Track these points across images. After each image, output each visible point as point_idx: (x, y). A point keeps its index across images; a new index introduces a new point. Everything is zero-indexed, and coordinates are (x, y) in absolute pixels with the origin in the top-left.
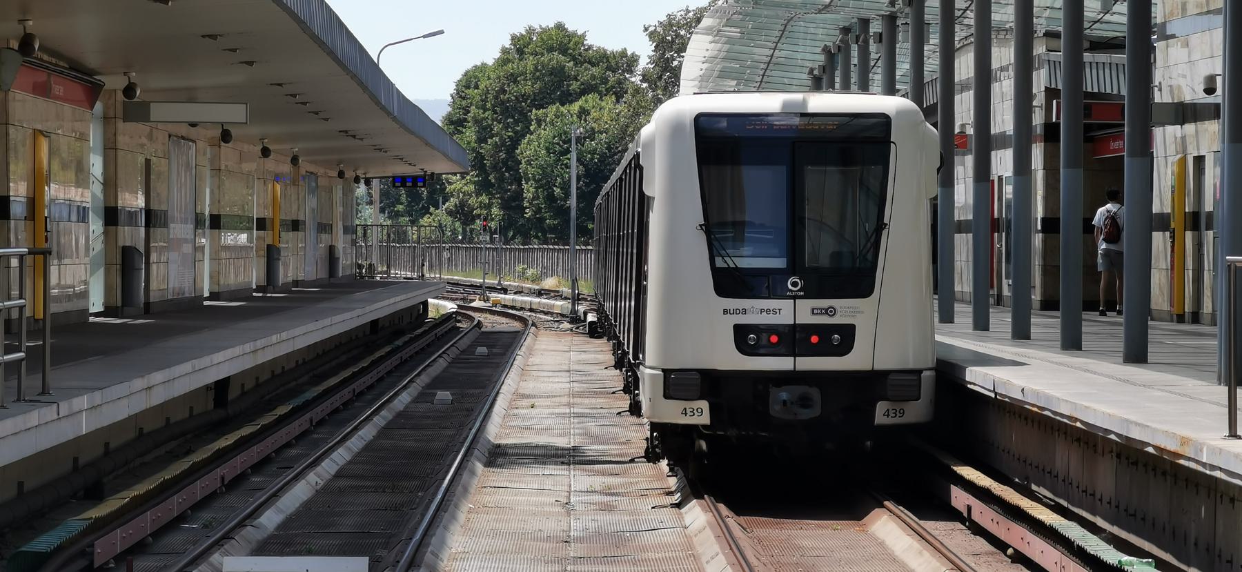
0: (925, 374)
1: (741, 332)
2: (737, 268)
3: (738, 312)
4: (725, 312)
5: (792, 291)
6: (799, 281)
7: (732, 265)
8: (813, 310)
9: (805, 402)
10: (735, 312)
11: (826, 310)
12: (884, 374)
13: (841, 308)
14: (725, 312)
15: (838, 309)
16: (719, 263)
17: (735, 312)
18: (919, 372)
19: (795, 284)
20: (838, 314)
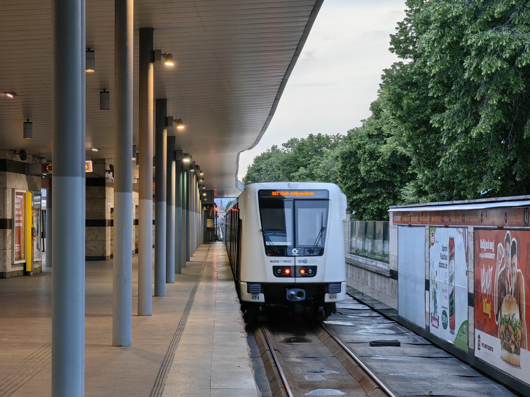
0: (343, 283)
1: (275, 268)
2: (273, 246)
3: (276, 261)
4: (271, 261)
5: (294, 254)
6: (296, 250)
7: (272, 245)
8: (299, 261)
9: (300, 294)
10: (275, 262)
11: (304, 261)
12: (327, 284)
13: (309, 260)
14: (271, 261)
15: (308, 260)
16: (268, 243)
17: (275, 262)
18: (340, 283)
19: (295, 251)
20: (308, 262)
